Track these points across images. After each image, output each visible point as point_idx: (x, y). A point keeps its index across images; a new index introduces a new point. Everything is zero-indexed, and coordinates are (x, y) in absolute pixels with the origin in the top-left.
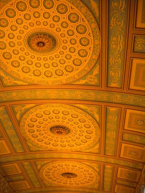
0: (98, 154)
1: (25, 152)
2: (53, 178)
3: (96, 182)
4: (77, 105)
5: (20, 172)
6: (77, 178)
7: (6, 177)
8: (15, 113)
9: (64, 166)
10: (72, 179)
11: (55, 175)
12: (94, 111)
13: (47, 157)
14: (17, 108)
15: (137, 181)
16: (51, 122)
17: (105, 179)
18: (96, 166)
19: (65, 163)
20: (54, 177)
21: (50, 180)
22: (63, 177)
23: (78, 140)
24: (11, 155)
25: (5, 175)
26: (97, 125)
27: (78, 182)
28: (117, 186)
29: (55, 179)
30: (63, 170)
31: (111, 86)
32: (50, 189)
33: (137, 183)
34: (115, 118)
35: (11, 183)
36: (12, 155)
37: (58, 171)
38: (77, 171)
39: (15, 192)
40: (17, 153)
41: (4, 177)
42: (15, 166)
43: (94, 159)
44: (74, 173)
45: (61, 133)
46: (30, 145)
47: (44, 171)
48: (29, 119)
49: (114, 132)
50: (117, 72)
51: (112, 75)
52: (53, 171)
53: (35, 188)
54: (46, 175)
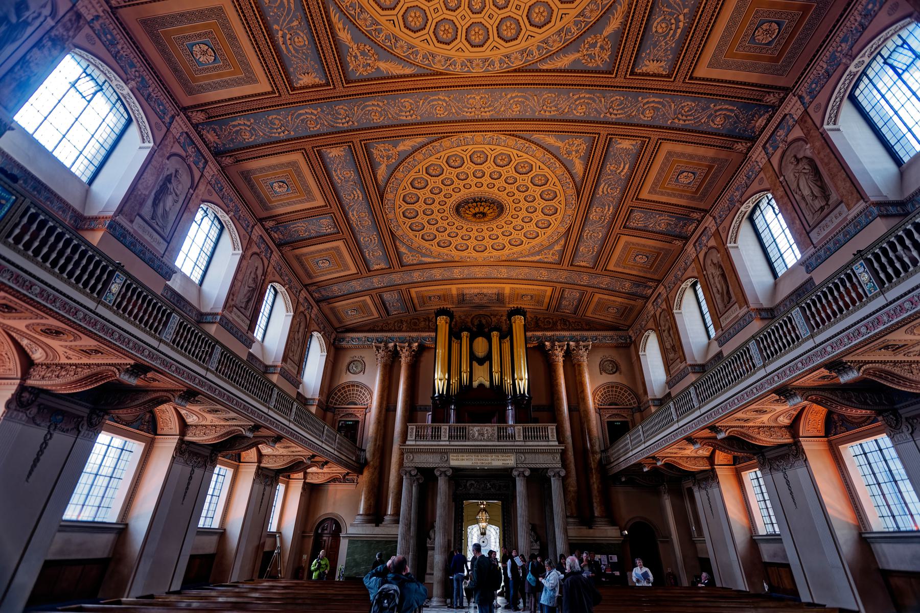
1: (390, 268)
4: (536, 136)
8: (373, 166)
12: (574, 153)
14: (379, 151)
16: (462, 188)
23: (517, 232)
26: (571, 191)
31: (644, 69)
34: (624, 168)
40: (370, 271)
45: (484, 215)
46: (403, 249)
48: (406, 183)
49: (611, 208)
50: (673, 21)
51: (656, 31)
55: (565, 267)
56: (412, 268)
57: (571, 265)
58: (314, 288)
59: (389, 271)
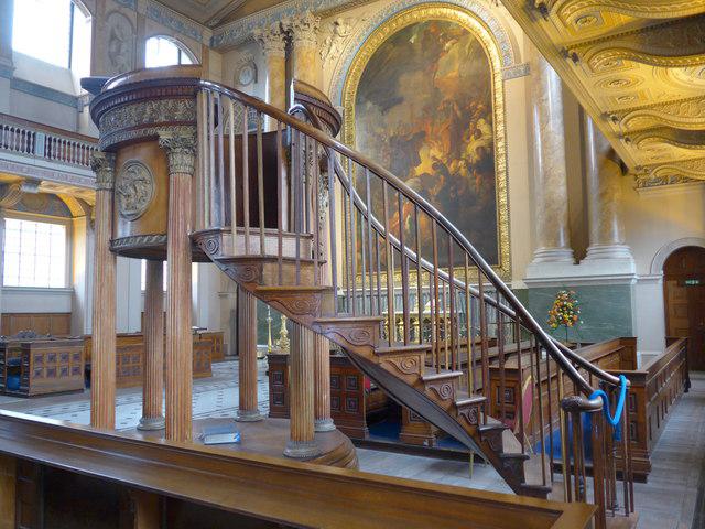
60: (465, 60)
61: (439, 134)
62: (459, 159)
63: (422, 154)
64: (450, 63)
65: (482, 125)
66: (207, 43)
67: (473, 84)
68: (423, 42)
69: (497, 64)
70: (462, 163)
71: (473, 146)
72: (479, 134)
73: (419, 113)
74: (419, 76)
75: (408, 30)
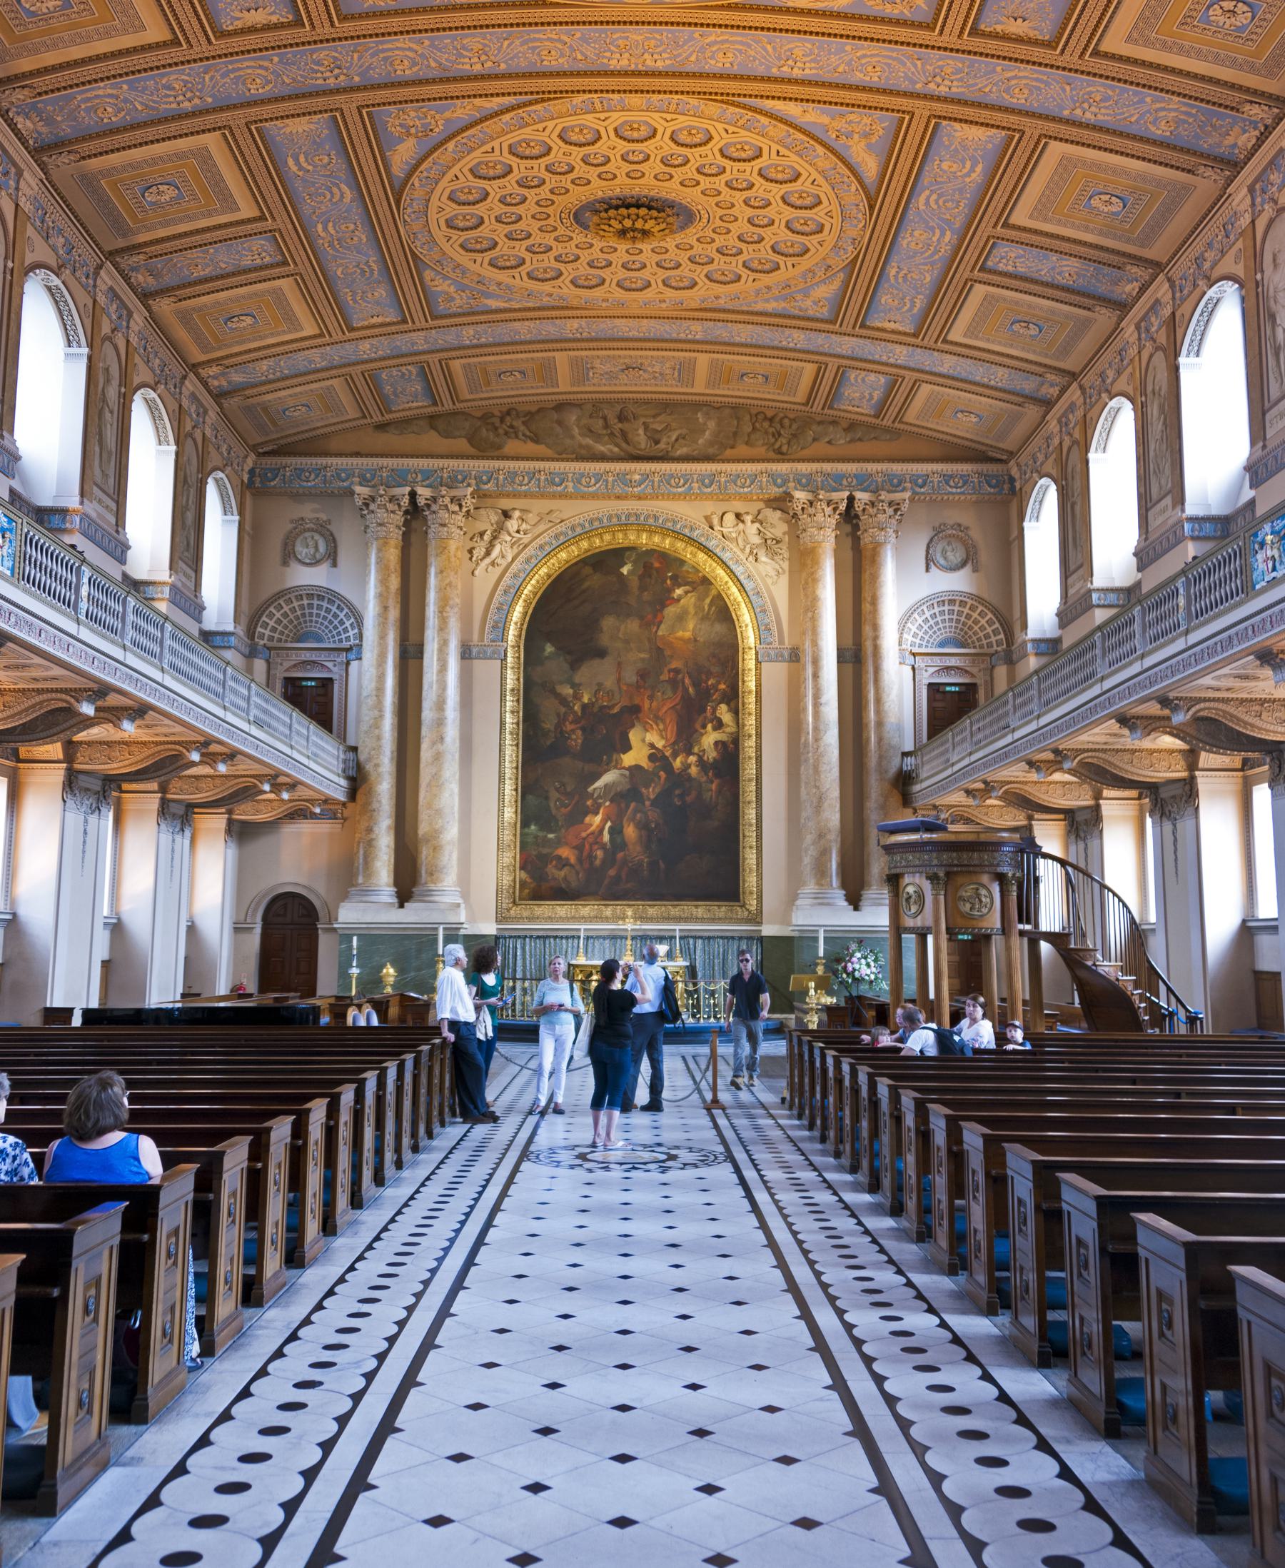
0: (920, 26)
1: (298, 23)
2: (502, 241)
3: (829, 262)
5: (247, 210)
6: (690, 236)
7: (127, 261)
9: (610, 145)
10: (646, 246)
11: (520, 218)
13: (477, 68)
15: (1156, 252)
17: (905, 242)
18: (866, 135)
19: (617, 118)
20: (509, 237)
21: (479, 266)
22: (579, 237)
24: (172, 54)
25: (121, 243)
27: (686, 271)
28: (980, 291)
29: (520, 249)
30: (592, 173)
32: (468, 335)
33: (1157, 267)
35: (164, 306)
36: (183, 52)
37: (552, 180)
38: (705, 182)
39: (197, 375)
41: (111, 255)
42: (203, 156)
43: (873, 79)
44: (672, 196)
47: (445, 184)
52: (510, 184)
53: (352, 329)
54: (449, 224)
55: (948, 39)
56: (382, 24)
57: (975, 32)
58: (20, 95)
59: (295, 34)
60: (705, 618)
61: (660, 714)
62: (690, 753)
63: (634, 736)
64: (681, 618)
65: (724, 712)
66: (246, 477)
67: (714, 656)
68: (641, 578)
69: (749, 637)
70: (692, 759)
71: (709, 739)
72: (719, 725)
73: (630, 676)
74: (633, 626)
75: (617, 555)
